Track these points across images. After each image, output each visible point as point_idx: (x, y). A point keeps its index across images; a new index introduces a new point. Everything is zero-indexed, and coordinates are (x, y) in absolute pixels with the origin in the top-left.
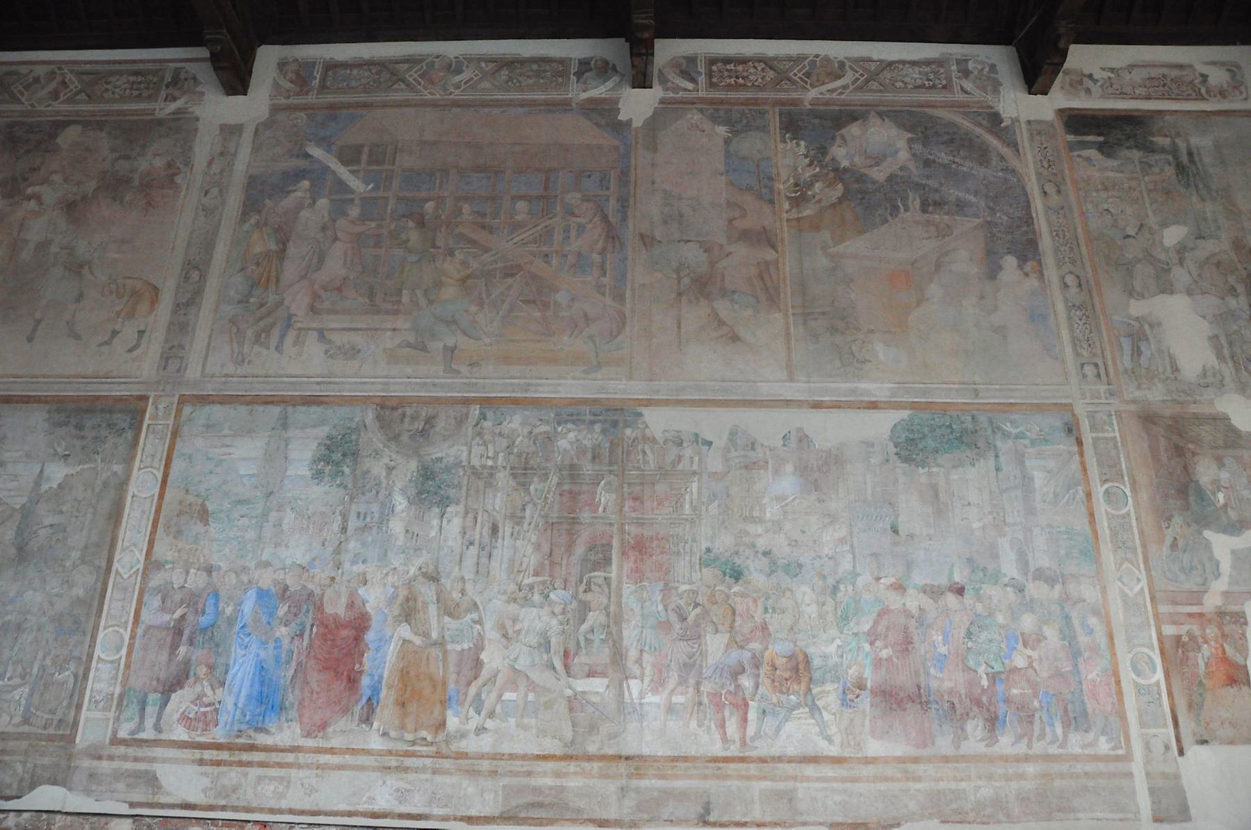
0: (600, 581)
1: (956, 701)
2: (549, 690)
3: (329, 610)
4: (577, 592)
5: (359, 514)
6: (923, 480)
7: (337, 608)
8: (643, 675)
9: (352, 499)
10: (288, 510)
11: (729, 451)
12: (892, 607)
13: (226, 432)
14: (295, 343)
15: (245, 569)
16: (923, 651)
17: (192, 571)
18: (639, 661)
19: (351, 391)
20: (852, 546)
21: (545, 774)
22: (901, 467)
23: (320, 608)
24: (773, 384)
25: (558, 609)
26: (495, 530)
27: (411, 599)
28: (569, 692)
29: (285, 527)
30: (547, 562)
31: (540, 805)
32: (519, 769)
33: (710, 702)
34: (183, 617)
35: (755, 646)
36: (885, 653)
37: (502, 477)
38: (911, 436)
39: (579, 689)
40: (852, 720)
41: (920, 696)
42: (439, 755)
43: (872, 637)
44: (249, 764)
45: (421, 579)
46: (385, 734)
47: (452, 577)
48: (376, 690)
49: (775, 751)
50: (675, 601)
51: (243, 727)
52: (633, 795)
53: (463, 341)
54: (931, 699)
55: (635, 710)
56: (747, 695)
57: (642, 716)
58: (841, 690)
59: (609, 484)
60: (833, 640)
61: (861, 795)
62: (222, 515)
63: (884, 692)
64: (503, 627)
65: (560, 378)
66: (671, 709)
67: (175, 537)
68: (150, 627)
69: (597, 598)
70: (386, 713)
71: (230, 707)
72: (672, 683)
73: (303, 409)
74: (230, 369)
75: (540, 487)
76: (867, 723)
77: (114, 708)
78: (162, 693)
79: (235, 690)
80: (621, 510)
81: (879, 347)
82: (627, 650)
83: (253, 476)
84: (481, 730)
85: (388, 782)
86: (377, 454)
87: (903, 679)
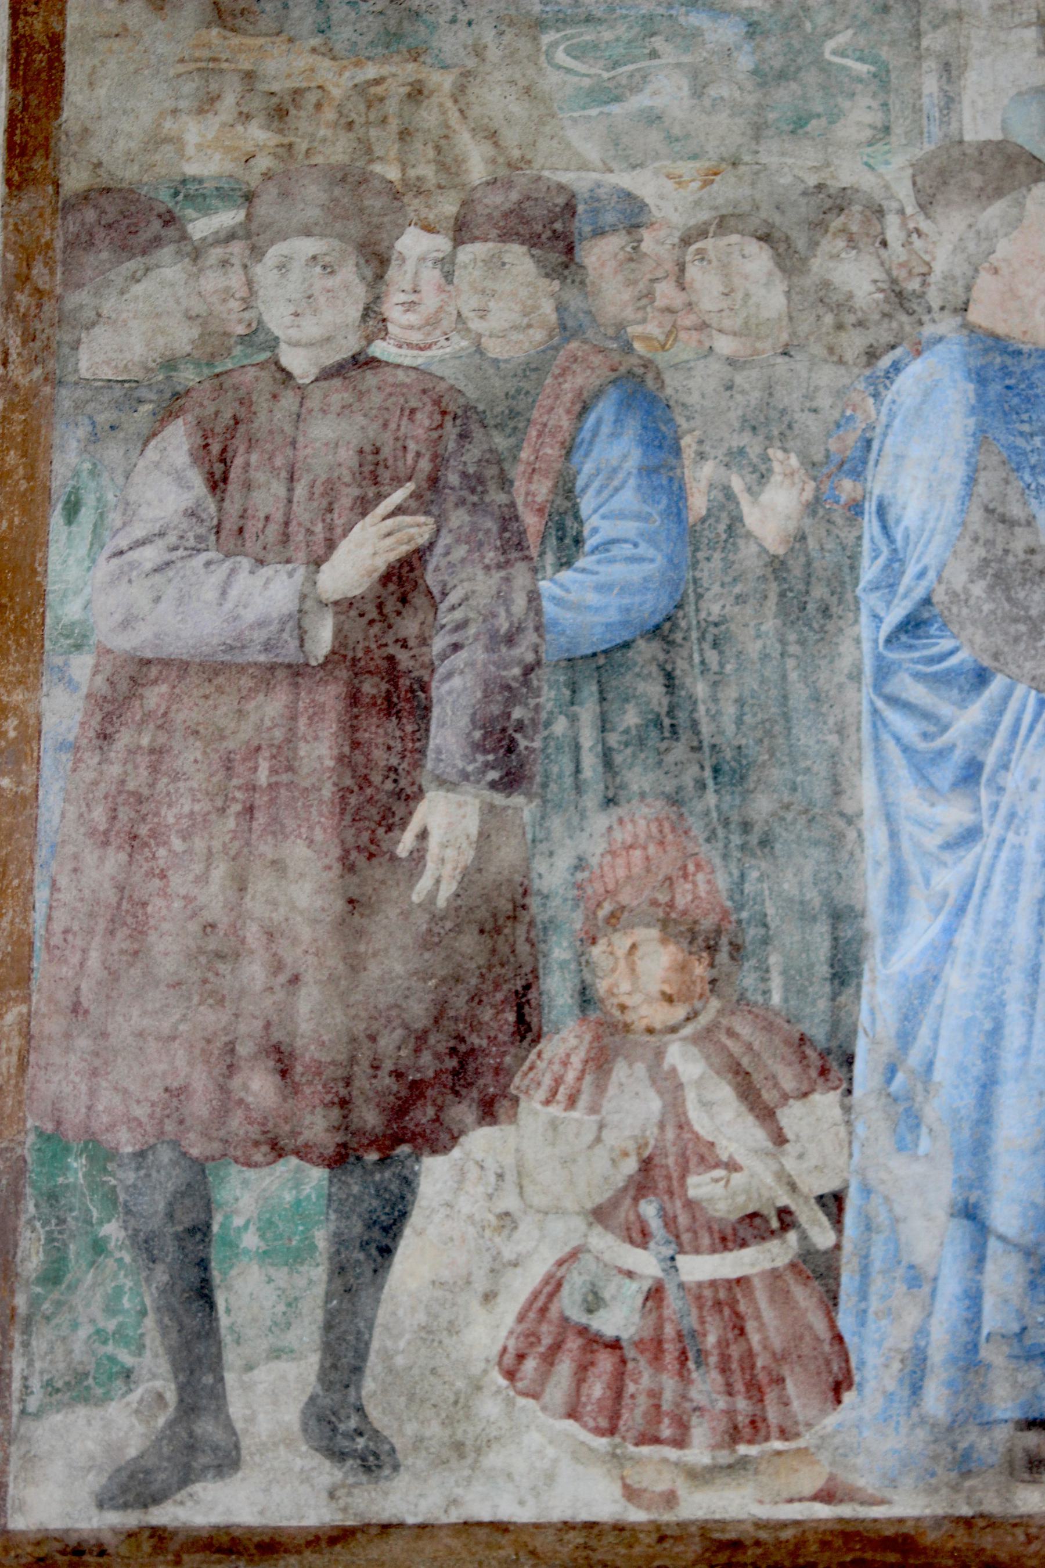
17: (414, 245)
34: (403, 579)
68: (140, 671)
71: (930, 1236)
78: (339, 1160)
79: (948, 1096)
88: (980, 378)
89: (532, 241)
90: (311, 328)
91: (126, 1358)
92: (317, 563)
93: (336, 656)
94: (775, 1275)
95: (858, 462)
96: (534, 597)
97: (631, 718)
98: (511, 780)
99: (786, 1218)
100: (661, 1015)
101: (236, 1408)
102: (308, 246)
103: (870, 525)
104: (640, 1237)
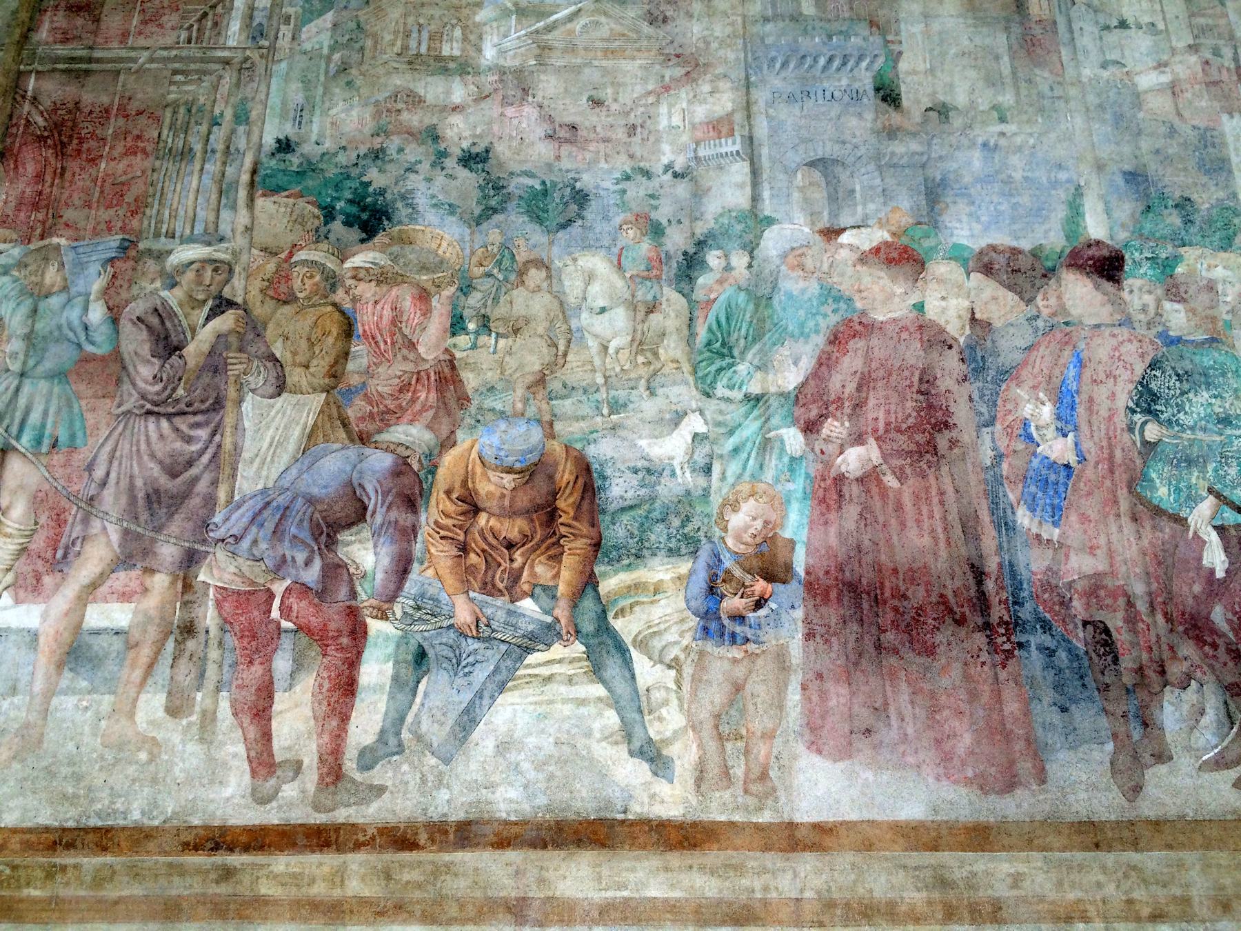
1: (1116, 621)
12: (879, 316)
16: (987, 456)
33: (226, 624)
35: (412, 434)
36: (853, 460)
40: (738, 688)
41: (982, 602)
43: (811, 407)
49: (448, 803)
50: (150, 291)
54: (1026, 613)
56: (365, 597)
60: (678, 418)
63: (853, 588)
66: (77, 652)
72: (95, 557)
76: (794, 696)
80: (25, 37)
87: (919, 542)
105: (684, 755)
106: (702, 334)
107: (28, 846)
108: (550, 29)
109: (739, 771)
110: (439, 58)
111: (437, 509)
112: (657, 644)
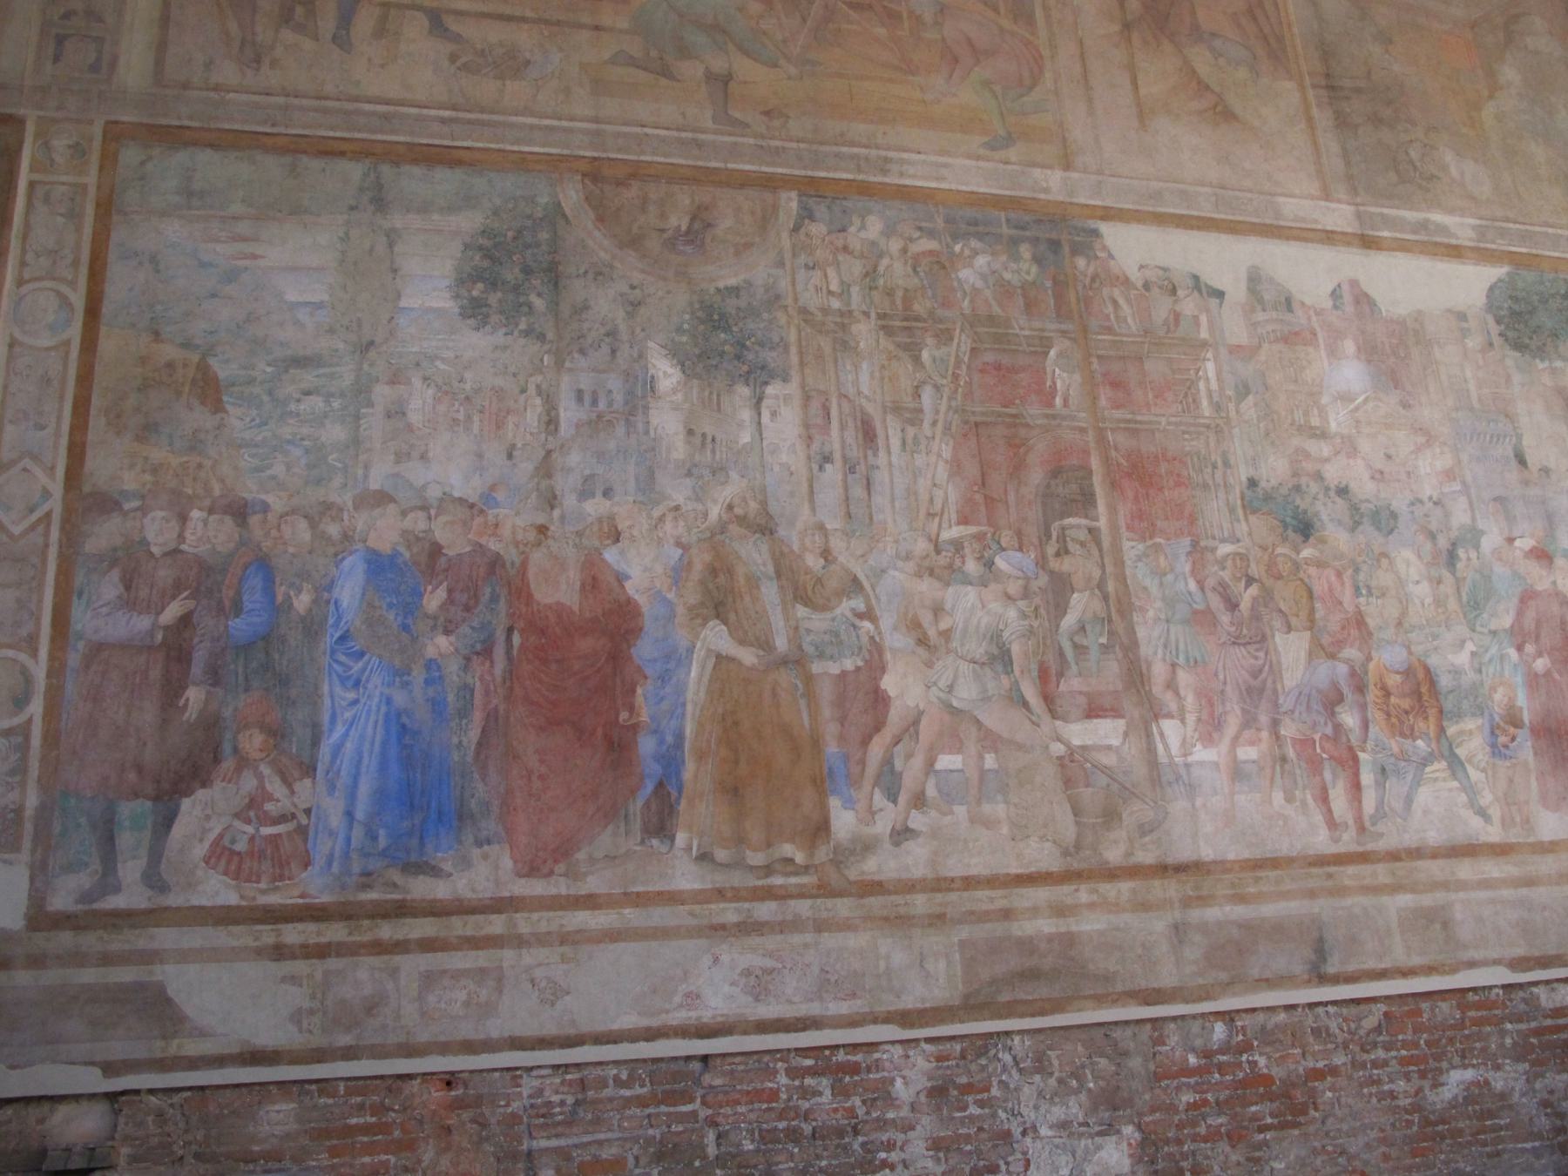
0: (1083, 535)
2: (1020, 747)
3: (544, 595)
4: (1044, 557)
5: (579, 396)
6: (1547, 380)
7: (558, 590)
8: (1182, 709)
9: (559, 364)
10: (417, 382)
11: (1253, 310)
12: (1539, 588)
13: (237, 208)
14: (380, 32)
15: (329, 509)
17: (196, 514)
18: (1171, 685)
19: (517, 142)
20: (1464, 483)
21: (1035, 912)
22: (1512, 357)
23: (520, 591)
24: (1299, 203)
25: (1014, 588)
26: (868, 435)
27: (721, 568)
28: (1058, 749)
29: (415, 418)
30: (979, 498)
31: (1032, 975)
32: (985, 907)
34: (185, 621)
35: (1351, 652)
36: (1541, 664)
37: (864, 332)
38: (1516, 307)
39: (1076, 742)
40: (1511, 781)
42: (824, 890)
44: (400, 947)
45: (734, 529)
46: (704, 857)
47: (800, 525)
48: (671, 761)
49: (1410, 840)
50: (1214, 574)
51: (375, 864)
52: (1197, 938)
53: (744, 67)
55: (1178, 778)
56: (1354, 742)
57: (1192, 789)
58: (1487, 730)
59: (1060, 355)
60: (1463, 642)
61: (1544, 908)
62: (257, 390)
64: (915, 625)
65: (943, 152)
66: (1237, 772)
67: (139, 439)
69: (1079, 565)
70: (700, 814)
71: (336, 821)
72: (1233, 724)
73: (417, 171)
74: (228, 72)
75: (937, 353)
76: (1534, 784)
77: (27, 844)
78: (156, 799)
79: (344, 778)
81: (1449, 157)
82: (1149, 665)
83: (320, 306)
84: (902, 834)
85: (725, 958)
86: (600, 274)
88: (369, 562)
89: (233, 515)
90: (161, 540)
91: (86, 859)
92: (158, 614)
93: (164, 643)
94: (289, 833)
95: (330, 587)
96: (227, 626)
97: (254, 665)
98: (215, 684)
99: (294, 816)
100: (258, 755)
101: (120, 873)
102: (160, 514)
103: (332, 607)
104: (249, 822)
105: (1495, 813)
106: (1465, 599)
107: (1242, 869)
108: (1357, 409)
109: (1518, 819)
110: (1311, 428)
111: (1373, 694)
112: (1476, 760)
